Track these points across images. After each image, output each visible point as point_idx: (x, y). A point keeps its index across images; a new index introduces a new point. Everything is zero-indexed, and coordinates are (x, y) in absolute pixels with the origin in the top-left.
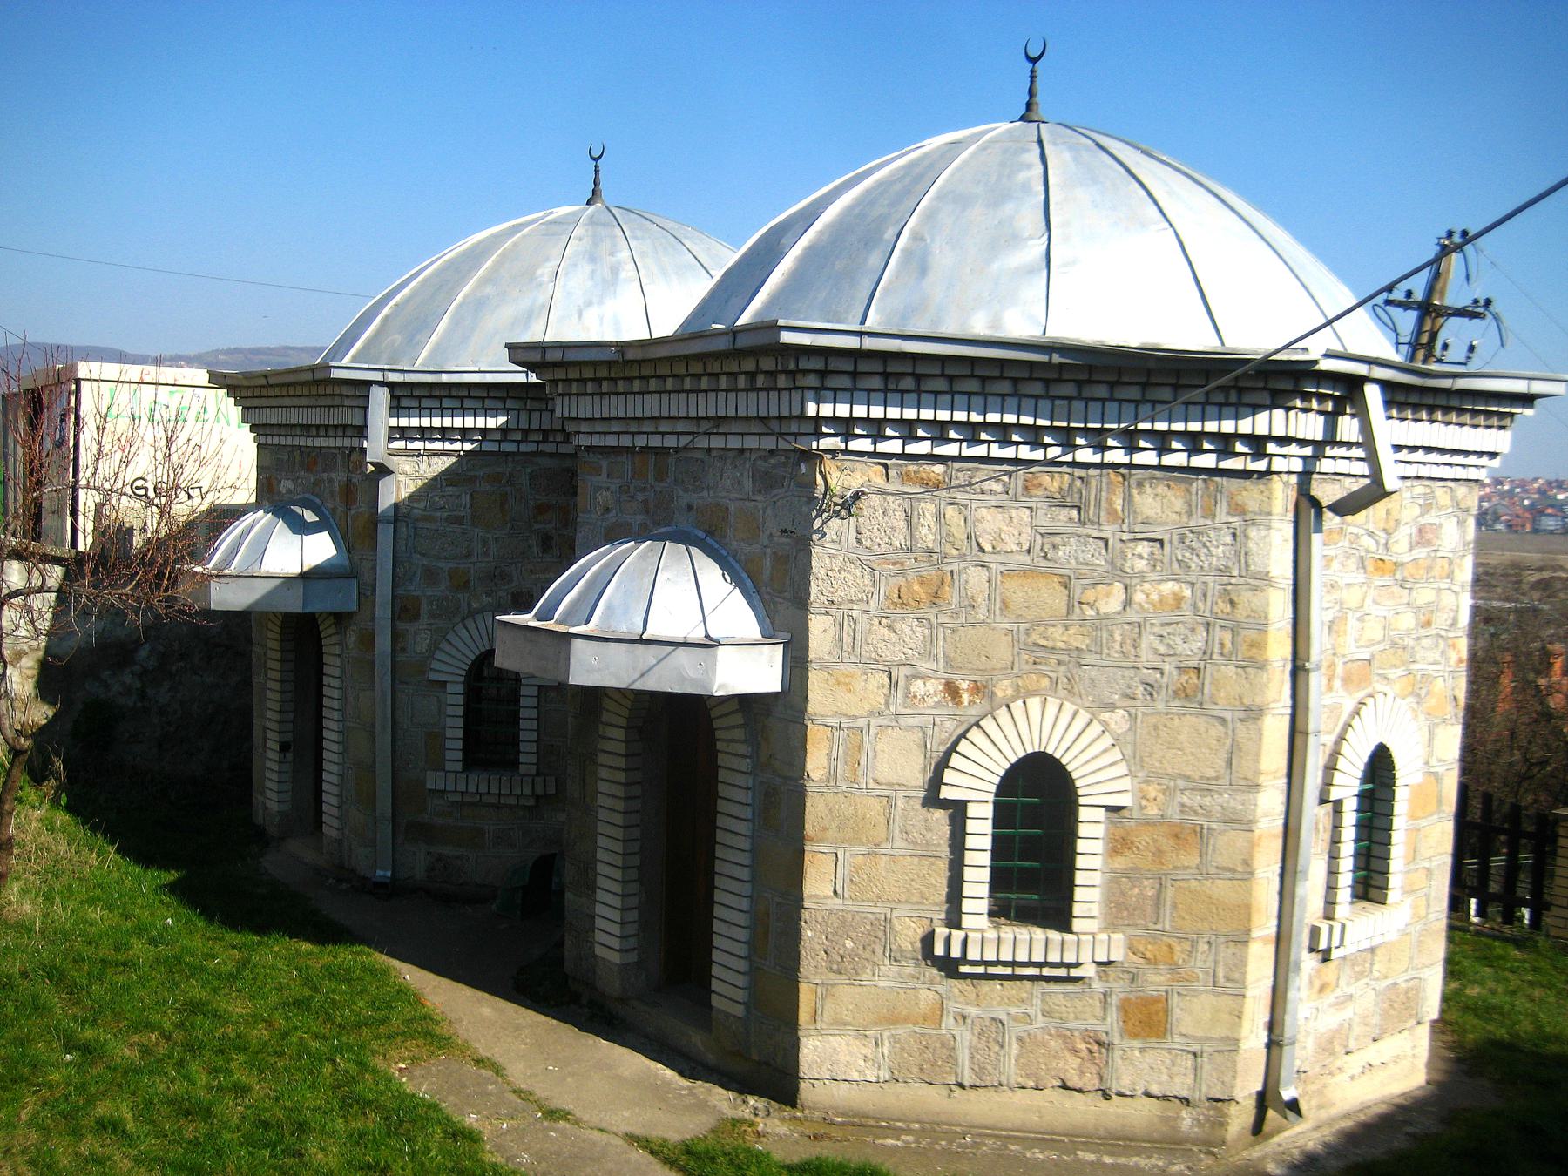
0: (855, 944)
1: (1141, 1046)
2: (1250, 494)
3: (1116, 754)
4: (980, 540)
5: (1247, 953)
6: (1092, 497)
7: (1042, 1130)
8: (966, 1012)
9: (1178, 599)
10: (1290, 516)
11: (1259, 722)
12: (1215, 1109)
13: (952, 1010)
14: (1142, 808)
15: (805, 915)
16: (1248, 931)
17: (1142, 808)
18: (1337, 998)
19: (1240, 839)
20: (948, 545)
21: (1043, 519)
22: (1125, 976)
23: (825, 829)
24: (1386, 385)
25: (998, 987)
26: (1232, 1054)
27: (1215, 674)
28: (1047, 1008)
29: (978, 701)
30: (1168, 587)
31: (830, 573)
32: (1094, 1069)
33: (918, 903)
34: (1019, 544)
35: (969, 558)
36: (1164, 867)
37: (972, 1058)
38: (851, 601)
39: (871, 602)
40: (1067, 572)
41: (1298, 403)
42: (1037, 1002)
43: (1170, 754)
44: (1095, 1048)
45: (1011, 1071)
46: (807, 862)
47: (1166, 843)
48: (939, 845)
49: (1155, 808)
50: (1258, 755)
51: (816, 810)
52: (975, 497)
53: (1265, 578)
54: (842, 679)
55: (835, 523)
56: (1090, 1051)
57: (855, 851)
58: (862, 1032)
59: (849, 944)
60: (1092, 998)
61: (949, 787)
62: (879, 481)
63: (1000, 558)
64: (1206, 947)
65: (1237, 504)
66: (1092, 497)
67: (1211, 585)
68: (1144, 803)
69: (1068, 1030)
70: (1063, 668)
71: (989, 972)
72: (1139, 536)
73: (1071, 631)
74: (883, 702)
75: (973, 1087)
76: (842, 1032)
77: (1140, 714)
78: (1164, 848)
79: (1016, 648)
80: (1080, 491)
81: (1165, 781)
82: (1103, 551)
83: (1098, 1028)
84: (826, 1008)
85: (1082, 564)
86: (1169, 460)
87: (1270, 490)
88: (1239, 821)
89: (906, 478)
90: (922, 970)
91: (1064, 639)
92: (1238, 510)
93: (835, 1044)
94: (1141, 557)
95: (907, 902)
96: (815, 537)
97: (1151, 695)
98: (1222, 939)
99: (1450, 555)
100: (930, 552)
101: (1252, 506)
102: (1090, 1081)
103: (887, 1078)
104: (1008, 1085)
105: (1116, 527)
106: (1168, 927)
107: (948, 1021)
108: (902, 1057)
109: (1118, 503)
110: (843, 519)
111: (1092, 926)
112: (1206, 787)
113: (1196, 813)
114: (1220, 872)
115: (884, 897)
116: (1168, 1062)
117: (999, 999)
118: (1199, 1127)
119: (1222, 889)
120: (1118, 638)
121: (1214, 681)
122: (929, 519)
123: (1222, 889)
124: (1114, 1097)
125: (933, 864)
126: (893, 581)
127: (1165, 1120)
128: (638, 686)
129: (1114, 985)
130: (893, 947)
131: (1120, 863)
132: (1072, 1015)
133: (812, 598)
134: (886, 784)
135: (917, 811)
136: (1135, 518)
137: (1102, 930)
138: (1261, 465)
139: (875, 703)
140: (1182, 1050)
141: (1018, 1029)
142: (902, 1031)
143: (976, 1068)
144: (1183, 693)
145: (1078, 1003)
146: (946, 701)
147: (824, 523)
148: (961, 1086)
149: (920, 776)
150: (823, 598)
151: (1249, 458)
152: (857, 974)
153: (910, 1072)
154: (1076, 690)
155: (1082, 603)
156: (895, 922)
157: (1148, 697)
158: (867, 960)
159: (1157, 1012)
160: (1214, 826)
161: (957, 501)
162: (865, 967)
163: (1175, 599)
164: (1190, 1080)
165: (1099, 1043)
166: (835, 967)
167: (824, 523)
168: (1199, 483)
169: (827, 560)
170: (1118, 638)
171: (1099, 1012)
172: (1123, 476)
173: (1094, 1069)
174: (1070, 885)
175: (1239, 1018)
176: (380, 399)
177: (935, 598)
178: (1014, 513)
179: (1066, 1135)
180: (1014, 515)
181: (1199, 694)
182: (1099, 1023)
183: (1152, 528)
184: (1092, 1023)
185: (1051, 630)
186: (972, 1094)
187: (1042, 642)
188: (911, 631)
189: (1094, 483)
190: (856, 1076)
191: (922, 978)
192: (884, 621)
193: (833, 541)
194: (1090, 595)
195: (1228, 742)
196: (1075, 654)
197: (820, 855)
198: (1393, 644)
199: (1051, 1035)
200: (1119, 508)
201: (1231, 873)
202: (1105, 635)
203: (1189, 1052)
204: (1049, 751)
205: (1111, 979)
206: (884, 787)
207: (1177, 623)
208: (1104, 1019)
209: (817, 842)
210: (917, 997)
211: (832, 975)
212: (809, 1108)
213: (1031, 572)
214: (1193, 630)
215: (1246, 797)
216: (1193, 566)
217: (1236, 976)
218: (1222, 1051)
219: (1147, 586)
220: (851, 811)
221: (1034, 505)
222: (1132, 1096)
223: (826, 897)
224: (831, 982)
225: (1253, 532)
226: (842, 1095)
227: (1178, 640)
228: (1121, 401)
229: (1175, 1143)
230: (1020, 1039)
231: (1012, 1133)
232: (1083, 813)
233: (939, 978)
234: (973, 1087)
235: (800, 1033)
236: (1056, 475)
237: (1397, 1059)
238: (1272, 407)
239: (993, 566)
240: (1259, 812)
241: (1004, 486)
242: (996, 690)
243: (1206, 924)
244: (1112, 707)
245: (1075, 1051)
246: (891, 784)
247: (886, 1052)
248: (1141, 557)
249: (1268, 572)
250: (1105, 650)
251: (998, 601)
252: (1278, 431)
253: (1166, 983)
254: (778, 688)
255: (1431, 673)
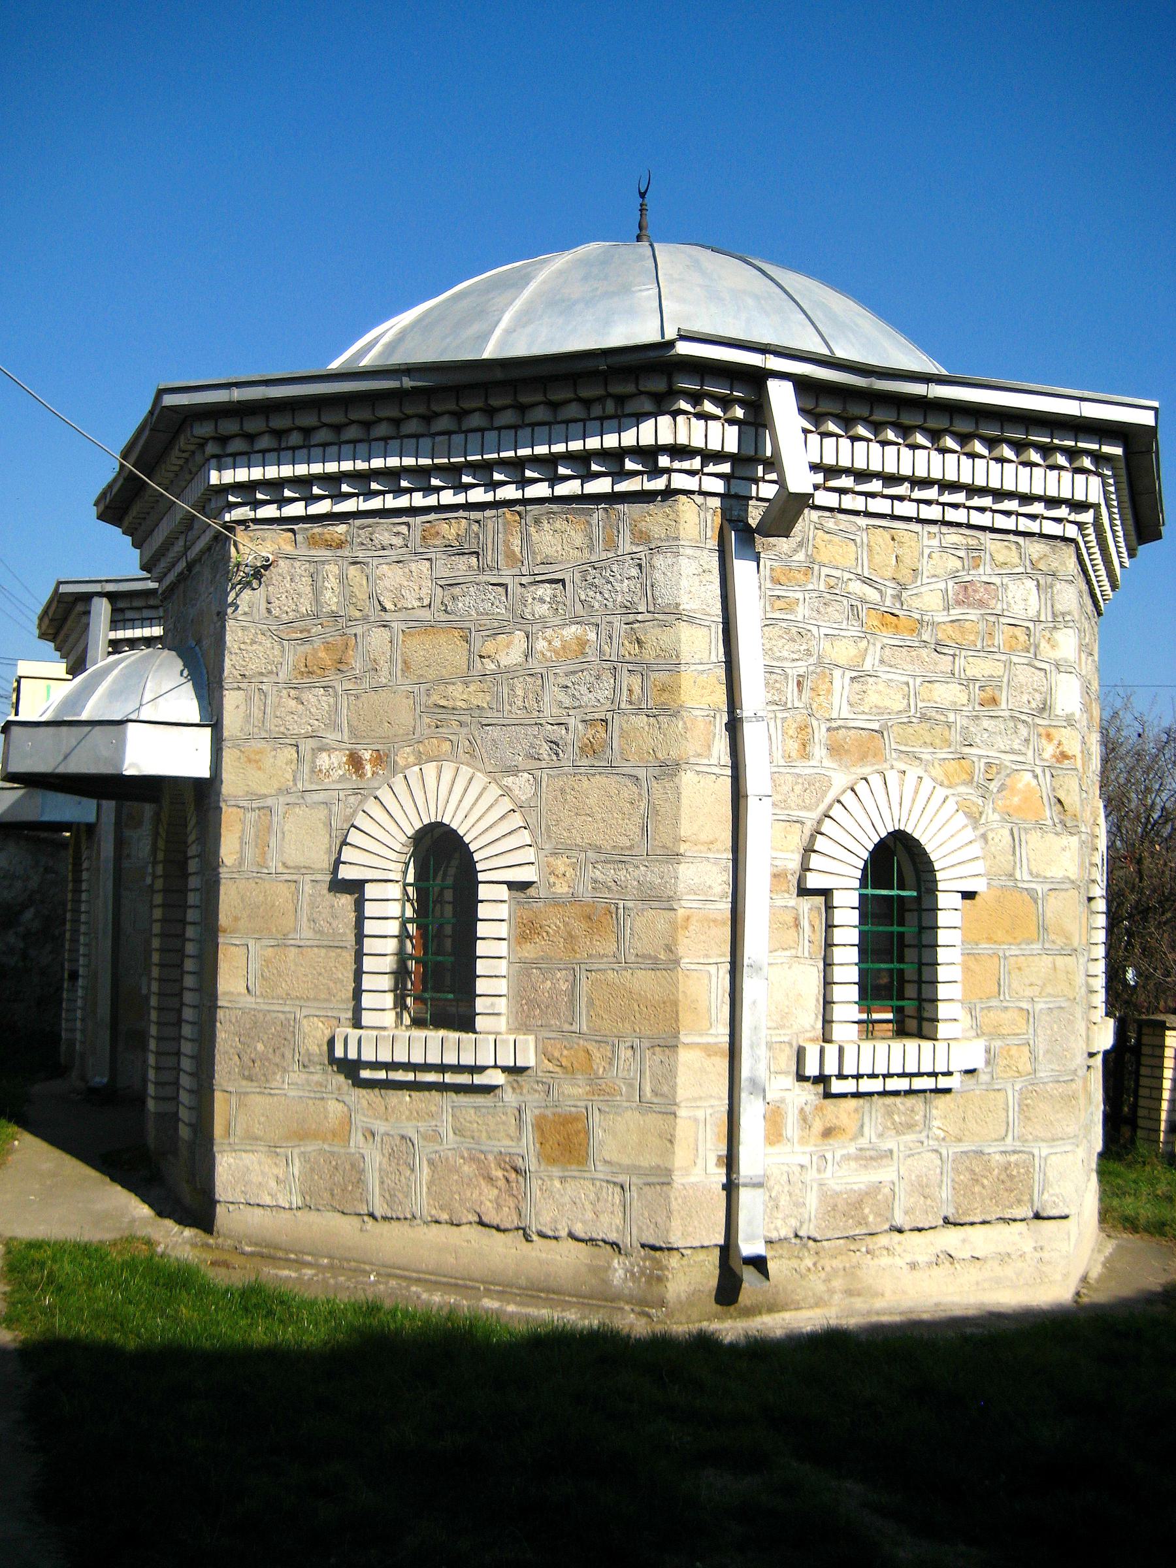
0: (265, 1047)
1: (561, 1174)
2: (653, 517)
3: (517, 820)
4: (382, 599)
5: (677, 1060)
6: (490, 540)
7: (458, 1275)
8: (375, 1128)
9: (582, 643)
10: (713, 543)
11: (676, 780)
12: (653, 1259)
13: (360, 1124)
14: (551, 885)
15: (220, 1014)
16: (676, 1036)
17: (551, 885)
18: (861, 1149)
19: (661, 921)
20: (352, 607)
21: (442, 571)
22: (540, 1087)
23: (236, 919)
24: (803, 385)
25: (408, 1098)
26: (665, 1188)
27: (625, 726)
28: (458, 1125)
29: (381, 772)
30: (573, 630)
31: (242, 646)
32: (511, 1203)
33: (326, 1000)
34: (420, 599)
35: (372, 619)
36: (578, 956)
37: (382, 1183)
38: (261, 674)
39: (280, 674)
40: (467, 625)
41: (684, 405)
42: (447, 1117)
43: (578, 822)
44: (513, 1176)
45: (421, 1201)
46: (221, 956)
47: (579, 927)
48: (344, 934)
49: (564, 884)
50: (676, 819)
51: (230, 898)
52: (376, 553)
53: (674, 614)
54: (252, 756)
55: (247, 594)
56: (507, 1180)
57: (265, 942)
58: (273, 1149)
59: (260, 1047)
60: (505, 1114)
61: (348, 865)
62: (289, 548)
63: (401, 615)
64: (630, 1053)
65: (641, 532)
66: (490, 540)
67: (617, 624)
68: (552, 879)
69: (482, 1152)
70: (464, 730)
71: (389, 1077)
72: (538, 578)
73: (472, 688)
74: (291, 778)
75: (385, 1218)
76: (254, 1148)
77: (545, 777)
78: (576, 932)
79: (418, 711)
80: (477, 535)
81: (574, 853)
82: (504, 598)
83: (513, 1151)
84: (239, 1119)
85: (482, 614)
86: (562, 489)
87: (676, 512)
88: (659, 899)
89: (312, 542)
90: (330, 1078)
91: (465, 697)
92: (641, 537)
93: (248, 1162)
94: (542, 601)
95: (316, 999)
96: (230, 610)
97: (557, 754)
98: (646, 1043)
99: (1031, 625)
100: (335, 616)
101: (657, 532)
102: (507, 1218)
103: (300, 1204)
104: (421, 1218)
105: (516, 571)
106: (585, 1029)
107: (357, 1139)
108: (312, 1180)
109: (516, 541)
110: (254, 589)
111: (502, 1024)
112: (621, 858)
113: (609, 888)
114: (640, 960)
115: (294, 994)
116: (592, 1196)
117: (407, 1113)
118: (634, 1282)
119: (643, 981)
120: (520, 692)
121: (623, 734)
122: (332, 582)
123: (643, 981)
124: (535, 1237)
125: (340, 956)
126: (301, 649)
127: (594, 1270)
128: (61, 770)
129: (529, 1098)
130: (302, 1051)
131: (529, 951)
132: (484, 1134)
133: (226, 673)
134: (294, 868)
135: (324, 896)
136: (534, 558)
137: (510, 1031)
138: (659, 484)
139: (283, 780)
140: (608, 1182)
141: (428, 1150)
142: (311, 1147)
143: (387, 1195)
144: (589, 749)
145: (491, 1121)
146: (351, 775)
147: (237, 595)
148: (372, 1215)
149: (326, 857)
150: (236, 673)
151: (645, 477)
152: (267, 1081)
153: (322, 1198)
154: (477, 753)
155: (484, 657)
156: (305, 1022)
157: (555, 758)
158: (277, 1065)
159: (578, 1132)
160: (630, 904)
161: (358, 560)
162: (274, 1073)
163: (579, 644)
164: (618, 1221)
165: (516, 1170)
166: (246, 1073)
167: (237, 595)
168: (598, 514)
169: (240, 633)
170: (520, 692)
171: (512, 1130)
172: (519, 513)
173: (511, 1203)
174: (471, 976)
175: (671, 1142)
176: (102, 610)
177: (340, 664)
178: (413, 566)
179: (483, 1282)
180: (413, 569)
181: (609, 751)
182: (514, 1144)
183: (551, 568)
184: (505, 1144)
185: (451, 688)
186: (384, 1227)
187: (443, 702)
188: (318, 700)
189: (490, 525)
190: (268, 1200)
191: (329, 1087)
192: (292, 692)
193: (245, 614)
194: (490, 647)
195: (643, 805)
196: (476, 713)
197: (233, 948)
198: (924, 718)
199: (463, 1157)
200: (517, 550)
201: (654, 964)
202: (506, 691)
203: (615, 1183)
204: (446, 821)
205: (525, 1091)
206: (292, 871)
207: (582, 671)
208: (519, 1139)
209: (230, 933)
210: (325, 1109)
211: (244, 1083)
212: (224, 1235)
213: (430, 628)
214: (598, 678)
215: (665, 868)
216: (597, 605)
217: (665, 1089)
218: (653, 1184)
219: (549, 632)
220: (261, 898)
221: (433, 556)
222: (556, 1238)
223: (239, 994)
224: (244, 1090)
225: (659, 561)
226: (255, 1220)
227: (584, 690)
228: (499, 429)
229: (606, 1300)
230: (431, 1163)
231: (422, 1276)
232: (483, 892)
233: (346, 1088)
234: (385, 1218)
235: (215, 1149)
236: (453, 521)
237: (1004, 1258)
238: (655, 415)
239: (393, 624)
240: (681, 887)
241: (404, 538)
242: (398, 759)
243: (627, 1025)
244: (514, 771)
245: (490, 1179)
246: (297, 868)
247: (296, 1173)
248: (542, 601)
249: (678, 605)
250: (507, 707)
251: (399, 661)
252: (665, 439)
253: (585, 1097)
254: (208, 776)
255: (1008, 764)
